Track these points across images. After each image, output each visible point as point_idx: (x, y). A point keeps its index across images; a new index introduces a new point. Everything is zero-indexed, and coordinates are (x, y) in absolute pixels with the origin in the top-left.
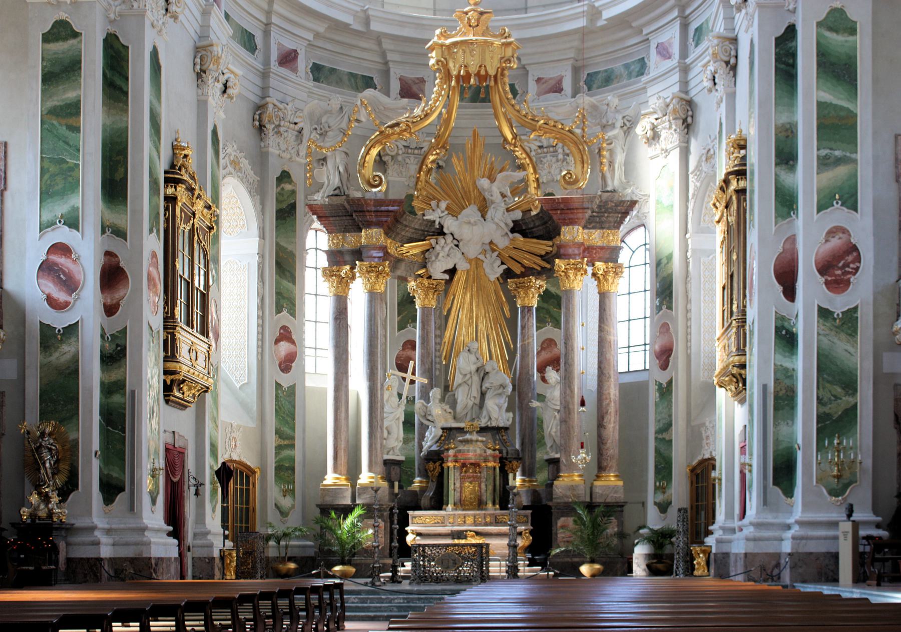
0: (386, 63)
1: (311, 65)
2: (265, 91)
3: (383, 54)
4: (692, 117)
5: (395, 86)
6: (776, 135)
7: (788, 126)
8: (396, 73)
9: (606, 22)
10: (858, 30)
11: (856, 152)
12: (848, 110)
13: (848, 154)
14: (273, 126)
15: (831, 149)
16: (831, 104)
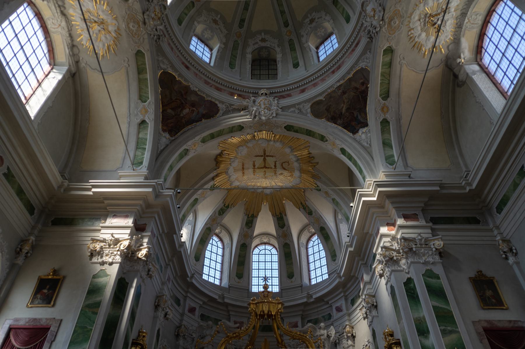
0: (229, 315)
1: (200, 314)
2: (181, 320)
3: (228, 311)
4: (355, 333)
6: (414, 322)
7: (419, 318)
8: (233, 319)
9: (314, 300)
10: (441, 277)
11: (458, 328)
12: (447, 309)
13: (454, 329)
14: (183, 335)
15: (445, 326)
16: (439, 307)
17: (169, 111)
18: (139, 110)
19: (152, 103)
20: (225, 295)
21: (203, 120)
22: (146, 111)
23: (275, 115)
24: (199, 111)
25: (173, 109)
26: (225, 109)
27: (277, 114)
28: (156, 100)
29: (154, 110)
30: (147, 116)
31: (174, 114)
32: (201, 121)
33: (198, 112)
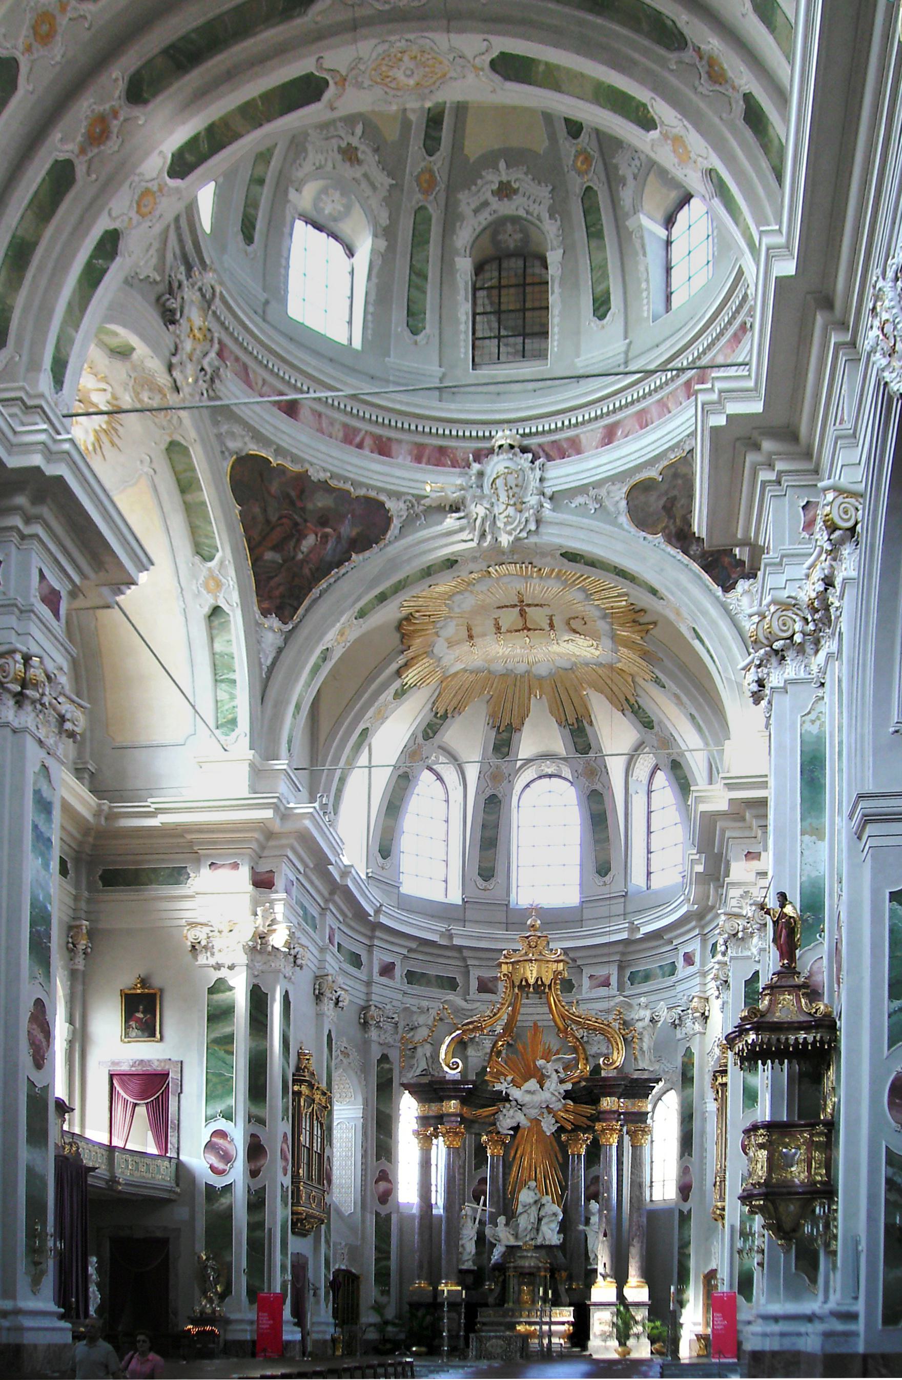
3: (464, 959)
5: (474, 984)
8: (474, 974)
17: (269, 555)
18: (201, 581)
19: (227, 562)
20: (453, 931)
21: (354, 556)
22: (219, 585)
23: (533, 527)
24: (340, 533)
25: (276, 548)
26: (405, 514)
27: (538, 522)
28: (235, 550)
29: (235, 579)
30: (221, 596)
31: (280, 561)
32: (349, 559)
33: (339, 537)
